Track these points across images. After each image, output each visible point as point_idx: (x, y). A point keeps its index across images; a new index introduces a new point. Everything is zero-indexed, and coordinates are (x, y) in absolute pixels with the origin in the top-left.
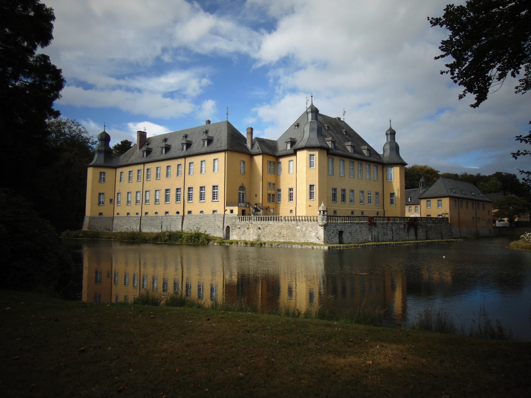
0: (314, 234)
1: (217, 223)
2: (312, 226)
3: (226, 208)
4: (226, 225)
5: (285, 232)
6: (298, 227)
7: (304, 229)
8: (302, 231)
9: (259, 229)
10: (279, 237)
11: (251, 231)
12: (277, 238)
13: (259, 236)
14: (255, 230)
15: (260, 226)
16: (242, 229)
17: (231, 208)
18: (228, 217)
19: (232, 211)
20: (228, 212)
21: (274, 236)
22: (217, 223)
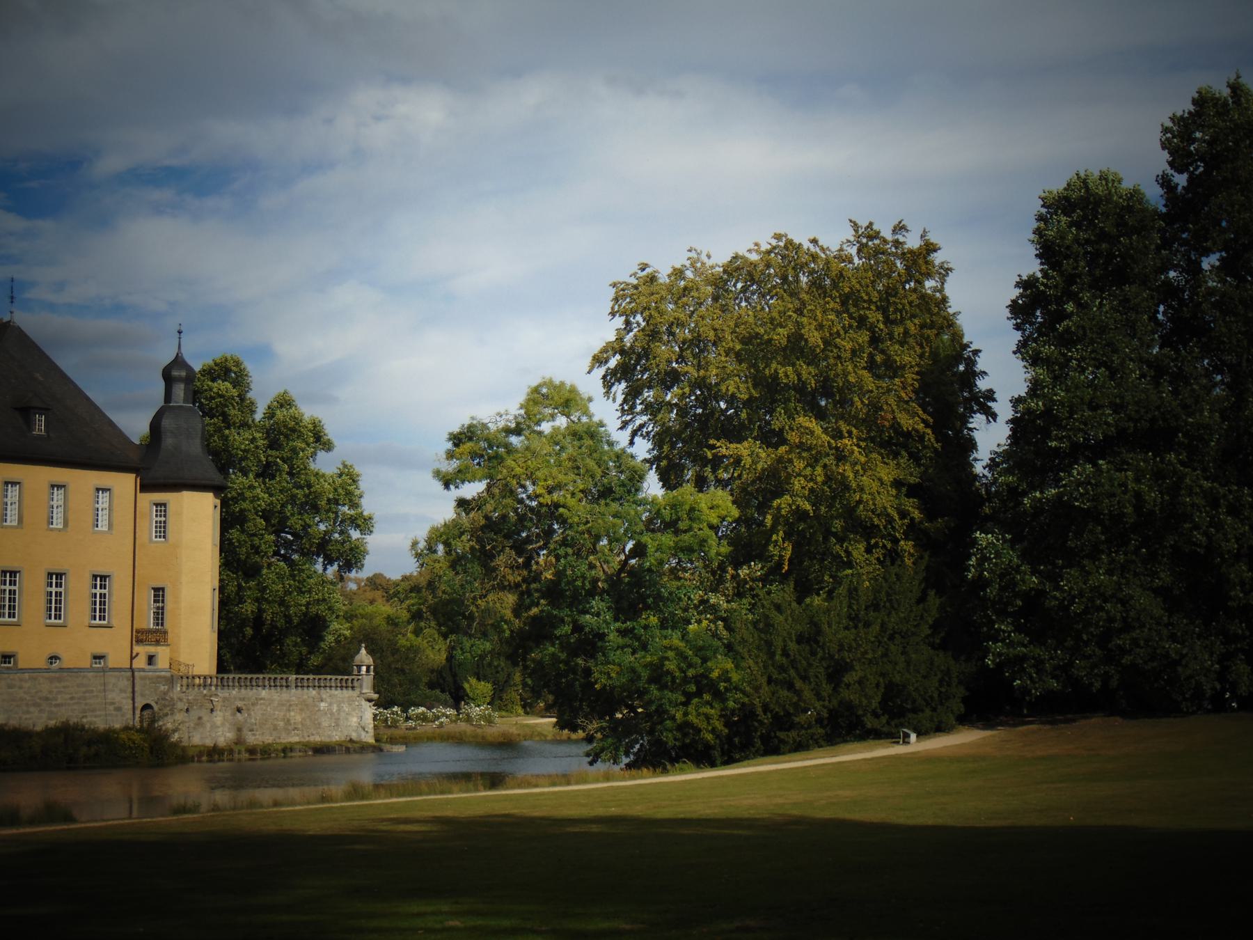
0: (355, 719)
1: (110, 696)
2: (350, 701)
3: (137, 649)
4: (139, 705)
5: (299, 718)
6: (323, 704)
7: (335, 708)
8: (332, 714)
9: (239, 710)
10: (288, 732)
11: (218, 717)
12: (284, 735)
13: (239, 730)
14: (228, 714)
15: (240, 704)
16: (194, 714)
17: (152, 649)
18: (142, 678)
19: (151, 659)
20: (141, 663)
21: (275, 728)
22: (110, 696)
